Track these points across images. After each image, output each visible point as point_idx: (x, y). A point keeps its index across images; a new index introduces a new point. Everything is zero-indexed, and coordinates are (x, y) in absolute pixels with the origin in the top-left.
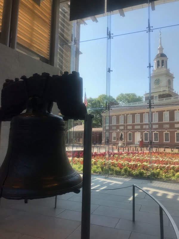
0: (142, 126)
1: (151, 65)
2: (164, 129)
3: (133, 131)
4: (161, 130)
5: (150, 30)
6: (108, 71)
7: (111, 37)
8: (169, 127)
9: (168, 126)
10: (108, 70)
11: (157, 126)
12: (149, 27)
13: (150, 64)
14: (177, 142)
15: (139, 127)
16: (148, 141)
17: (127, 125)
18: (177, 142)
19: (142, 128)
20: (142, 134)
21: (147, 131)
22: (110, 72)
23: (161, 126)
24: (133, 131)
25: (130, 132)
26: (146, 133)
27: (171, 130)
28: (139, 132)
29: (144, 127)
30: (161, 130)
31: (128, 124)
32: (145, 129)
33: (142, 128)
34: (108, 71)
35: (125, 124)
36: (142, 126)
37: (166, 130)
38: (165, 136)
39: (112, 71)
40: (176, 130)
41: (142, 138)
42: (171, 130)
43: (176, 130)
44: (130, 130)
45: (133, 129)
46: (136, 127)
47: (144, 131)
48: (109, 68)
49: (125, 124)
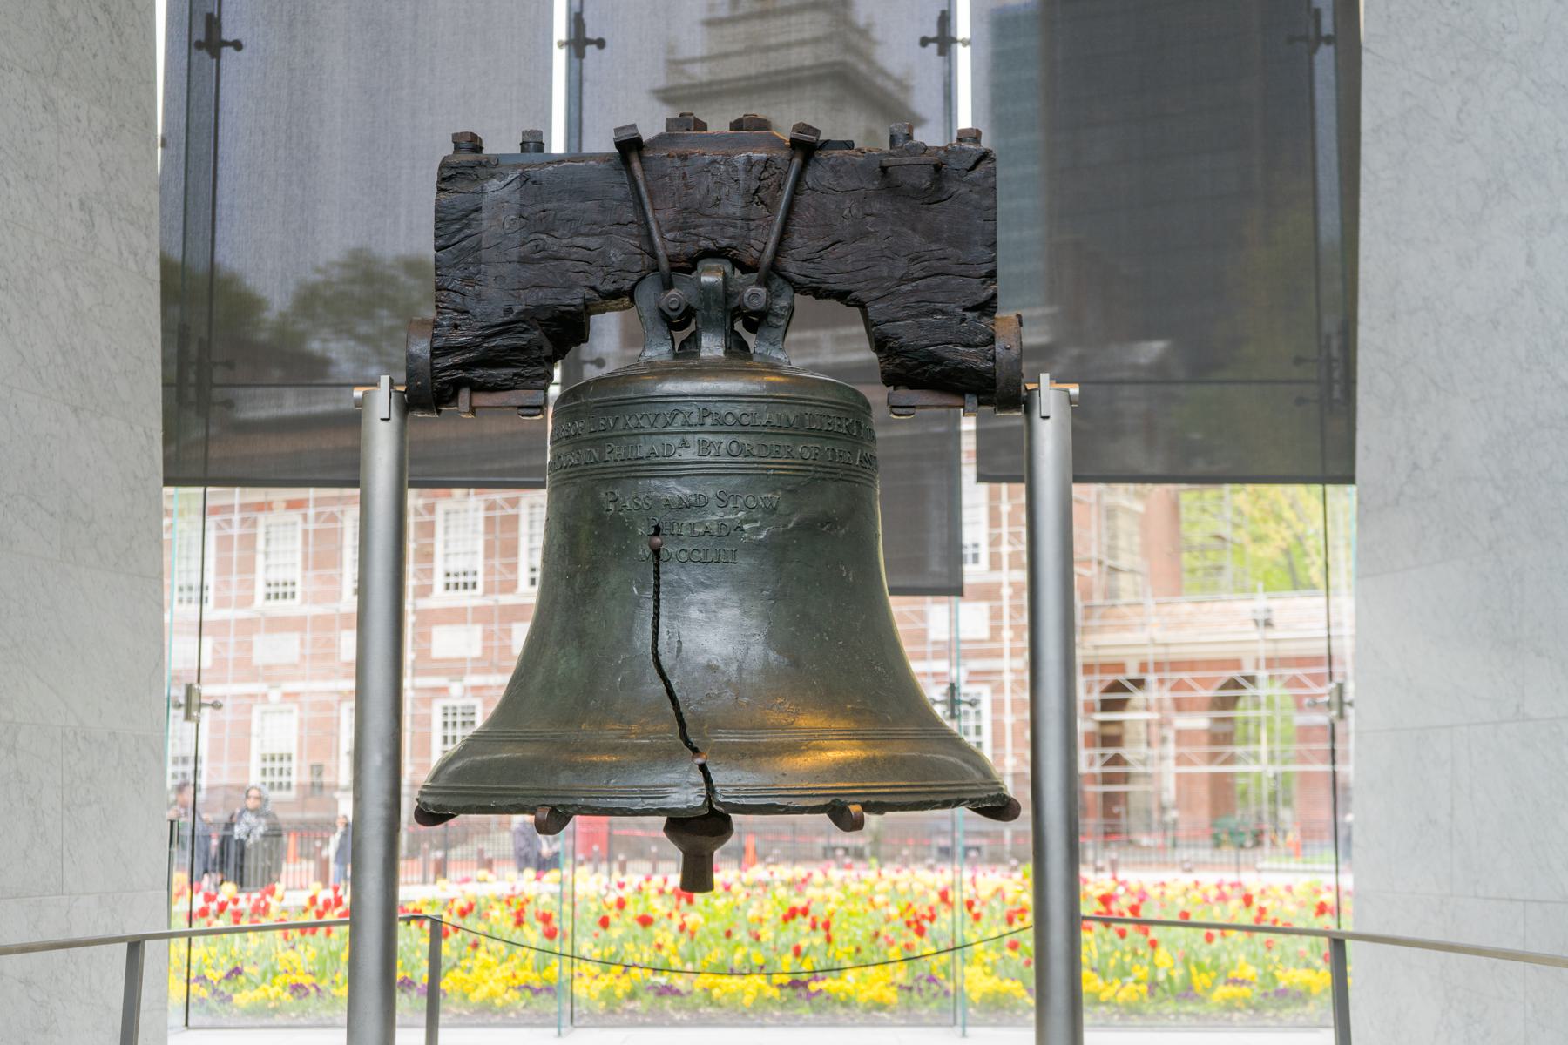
6: (199, 45)
10: (200, 34)
22: (216, 55)
25: (456, 689)
34: (199, 45)
48: (209, 17)
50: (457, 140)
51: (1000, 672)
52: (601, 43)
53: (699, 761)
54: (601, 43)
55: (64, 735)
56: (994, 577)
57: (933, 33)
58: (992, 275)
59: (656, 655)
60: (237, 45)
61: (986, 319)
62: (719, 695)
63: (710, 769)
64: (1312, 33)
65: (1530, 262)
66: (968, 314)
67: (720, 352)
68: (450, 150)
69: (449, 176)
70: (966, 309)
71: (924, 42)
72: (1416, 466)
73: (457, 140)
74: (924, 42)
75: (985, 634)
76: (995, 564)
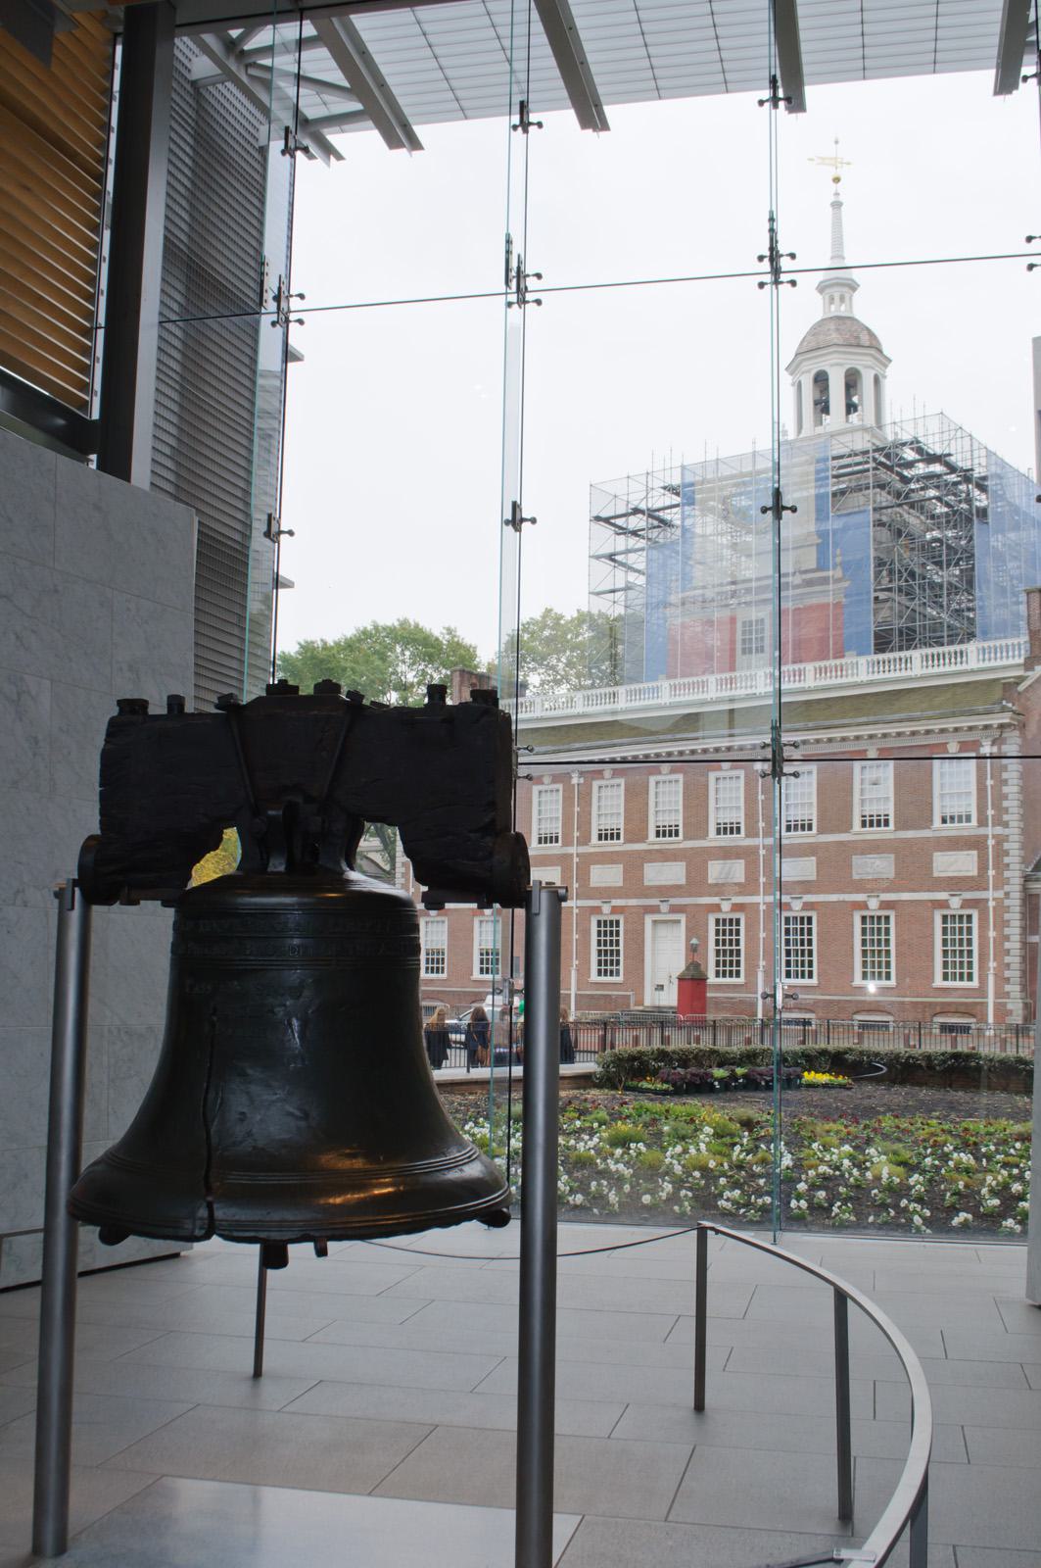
0: (697, 862)
2: (859, 886)
3: (633, 902)
4: (834, 898)
5: (521, 291)
7: (292, 317)
8: (892, 875)
9: (881, 866)
12: (517, 279)
13: (515, 506)
14: (949, 984)
15: (673, 873)
17: (587, 861)
18: (949, 984)
19: (696, 881)
20: (695, 929)
24: (633, 902)
27: (906, 896)
28: (674, 909)
29: (715, 871)
30: (834, 898)
31: (595, 845)
32: (719, 889)
33: (696, 881)
35: (573, 850)
36: (697, 862)
38: (717, 942)
39: (291, 533)
40: (942, 896)
42: (906, 896)
43: (942, 896)
44: (606, 893)
45: (633, 884)
46: (657, 874)
47: (715, 900)
49: (573, 850)
50: (123, 704)
51: (987, 900)
52: (533, 521)
53: (210, 1199)
54: (533, 521)
55: (110, 1031)
56: (982, 831)
57: (769, 503)
58: (492, 805)
59: (205, 1106)
61: (488, 839)
62: (241, 1142)
63: (215, 1206)
66: (472, 835)
67: (282, 868)
68: (115, 711)
69: (114, 728)
70: (471, 832)
71: (764, 510)
73: (119, 702)
74: (764, 510)
75: (975, 873)
76: (983, 822)
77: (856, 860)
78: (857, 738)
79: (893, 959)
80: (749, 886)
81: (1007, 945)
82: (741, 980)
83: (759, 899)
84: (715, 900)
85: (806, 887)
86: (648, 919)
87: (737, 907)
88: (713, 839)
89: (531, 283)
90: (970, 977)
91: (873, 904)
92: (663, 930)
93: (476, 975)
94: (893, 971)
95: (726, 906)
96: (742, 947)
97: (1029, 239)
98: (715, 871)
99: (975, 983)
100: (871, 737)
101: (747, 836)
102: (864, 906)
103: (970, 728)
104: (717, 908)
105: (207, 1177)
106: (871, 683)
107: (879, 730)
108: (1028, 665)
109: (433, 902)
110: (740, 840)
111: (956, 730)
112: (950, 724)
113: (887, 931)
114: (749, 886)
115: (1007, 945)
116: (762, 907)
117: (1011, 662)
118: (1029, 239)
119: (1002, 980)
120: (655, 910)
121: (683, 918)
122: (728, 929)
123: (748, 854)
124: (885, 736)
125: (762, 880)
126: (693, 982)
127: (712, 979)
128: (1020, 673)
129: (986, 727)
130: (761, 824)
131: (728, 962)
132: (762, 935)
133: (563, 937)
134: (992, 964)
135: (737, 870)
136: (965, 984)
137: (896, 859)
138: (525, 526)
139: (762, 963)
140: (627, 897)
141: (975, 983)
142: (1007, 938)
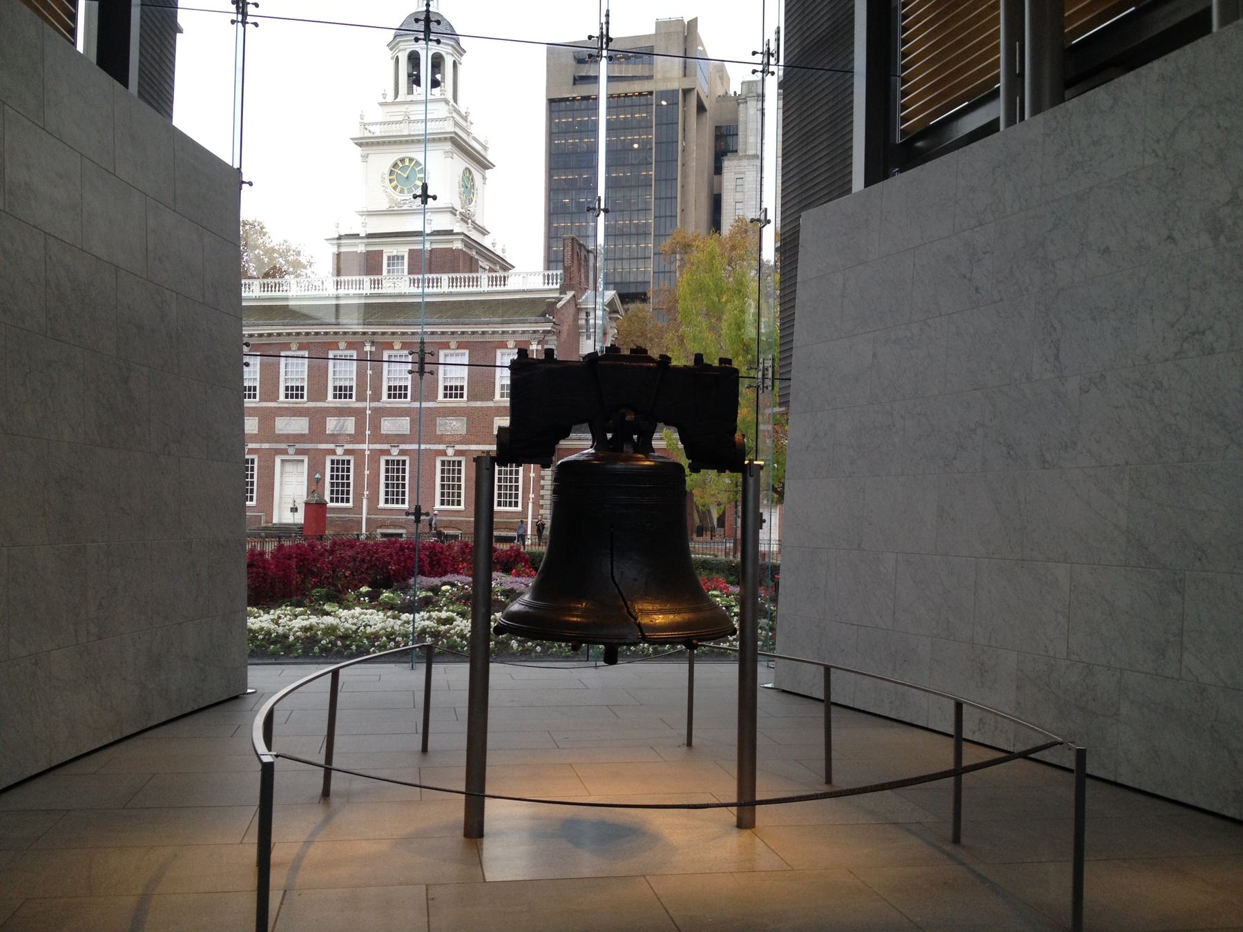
0: (317, 418)
1: (429, 193)
2: (440, 439)
5: (427, 31)
8: (464, 432)
11: (403, 425)
15: (300, 425)
16: (406, 506)
19: (317, 432)
21: (348, 447)
23: (423, 424)
26: (341, 458)
27: (474, 447)
28: (298, 452)
29: (332, 424)
32: (334, 438)
33: (317, 432)
36: (317, 418)
37: (451, 444)
39: (251, 184)
41: (315, 484)
42: (474, 447)
46: (284, 425)
47: (331, 446)
60: (251, 184)
64: (763, 217)
65: (875, 356)
72: (816, 436)
77: (439, 421)
78: (443, 333)
79: (463, 491)
80: (358, 437)
81: (542, 482)
82: (350, 505)
83: (365, 446)
84: (331, 446)
85: (401, 438)
86: (278, 460)
87: (347, 452)
88: (331, 401)
89: (433, 26)
90: (516, 504)
91: (450, 451)
92: (289, 467)
93: (438, 506)
94: (462, 499)
95: (339, 451)
96: (351, 481)
97: (754, 53)
98: (332, 424)
99: (519, 508)
100: (453, 333)
101: (357, 400)
102: (444, 453)
103: (524, 332)
104: (333, 452)
105: (629, 613)
106: (450, 294)
107: (459, 329)
108: (563, 290)
109: (695, 469)
110: (352, 403)
111: (514, 332)
112: (510, 329)
113: (459, 471)
114: (358, 437)
115: (542, 482)
116: (367, 453)
117: (551, 286)
118: (754, 53)
119: (537, 506)
120: (285, 452)
121: (306, 459)
122: (340, 467)
123: (358, 413)
124: (463, 333)
125: (368, 432)
126: (315, 509)
127: (330, 505)
128: (557, 295)
129: (534, 332)
130: (369, 392)
131: (340, 491)
132: (367, 472)
133: (473, 475)
134: (532, 496)
135: (350, 425)
136: (513, 509)
137: (468, 420)
138: (430, 200)
139: (366, 493)
140: (262, 442)
141: (519, 508)
142: (543, 478)
